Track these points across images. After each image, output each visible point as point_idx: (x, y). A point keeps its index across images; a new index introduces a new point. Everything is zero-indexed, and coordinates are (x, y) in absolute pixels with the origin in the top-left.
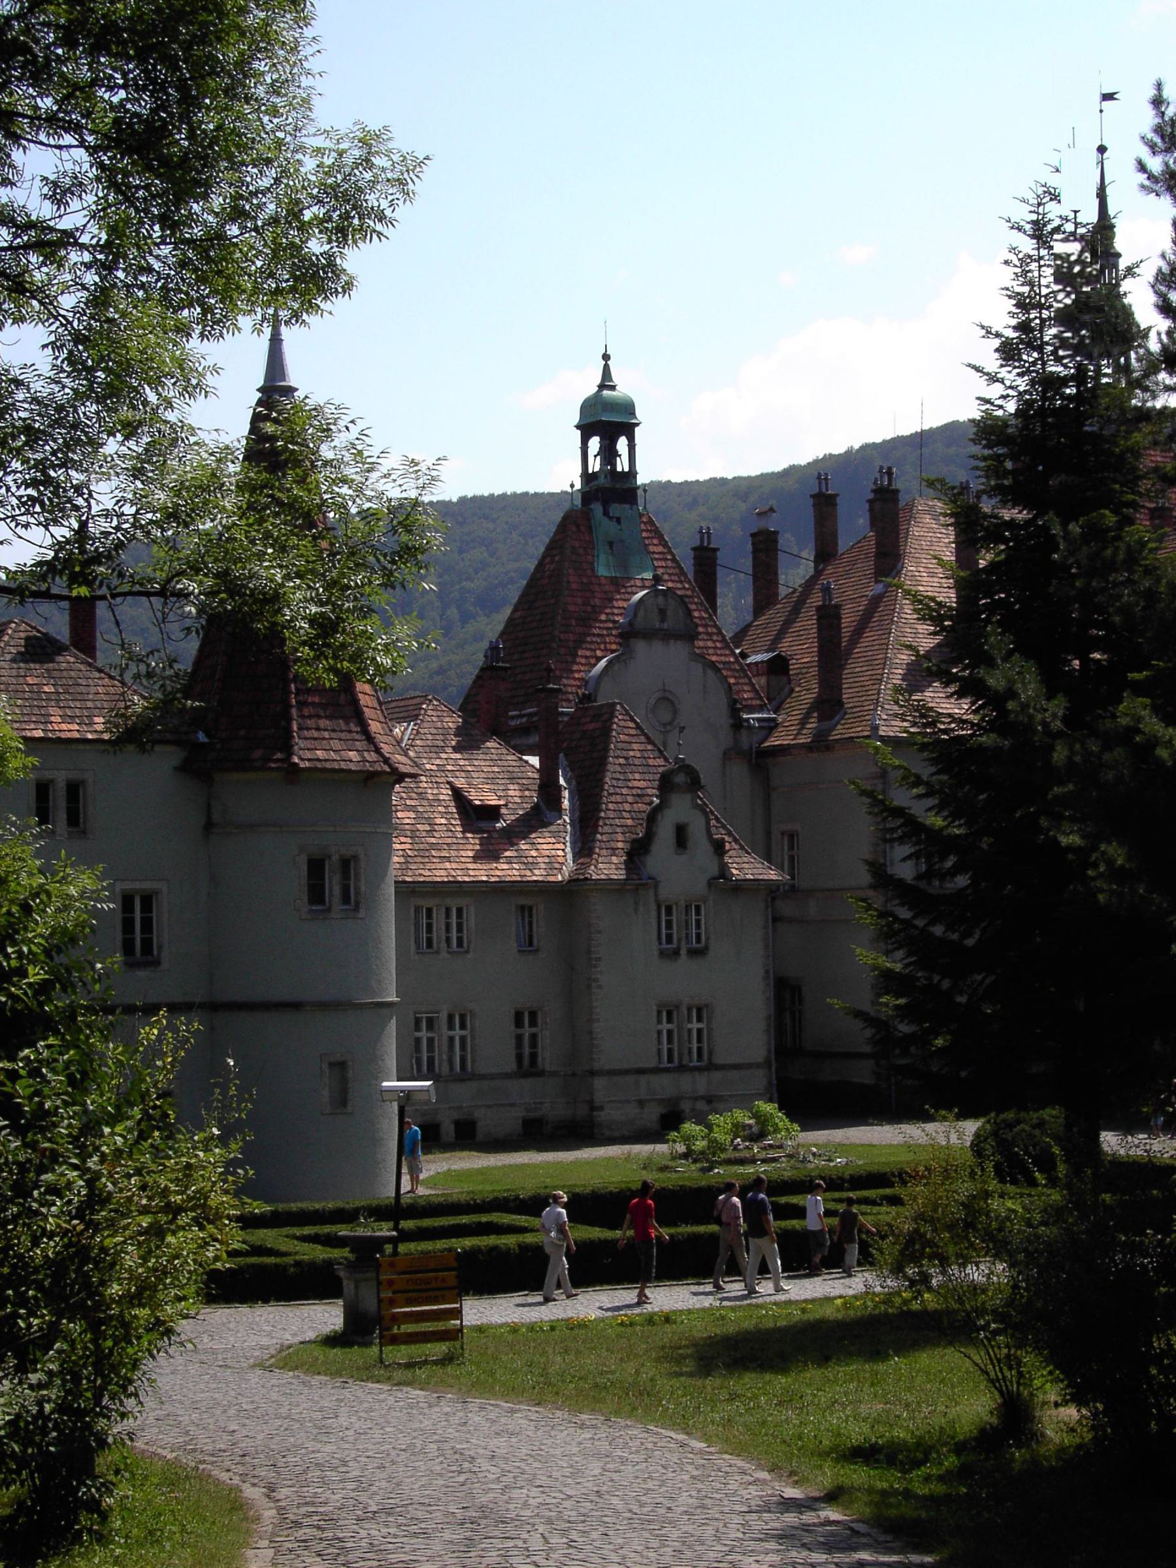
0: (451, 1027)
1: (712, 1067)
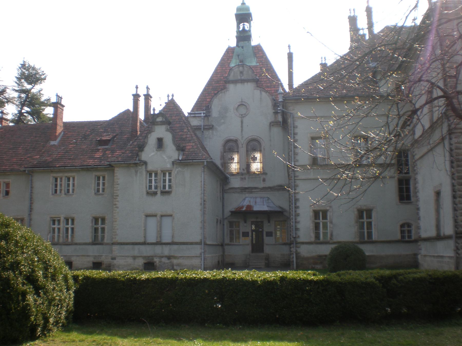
0: (67, 224)
1: (173, 243)
